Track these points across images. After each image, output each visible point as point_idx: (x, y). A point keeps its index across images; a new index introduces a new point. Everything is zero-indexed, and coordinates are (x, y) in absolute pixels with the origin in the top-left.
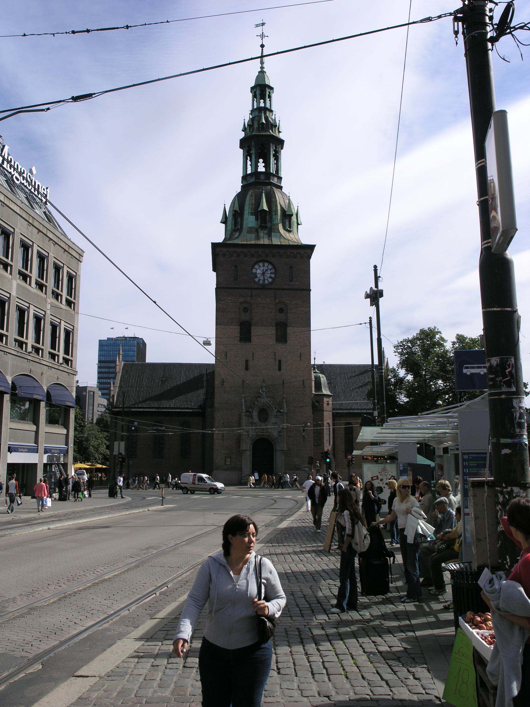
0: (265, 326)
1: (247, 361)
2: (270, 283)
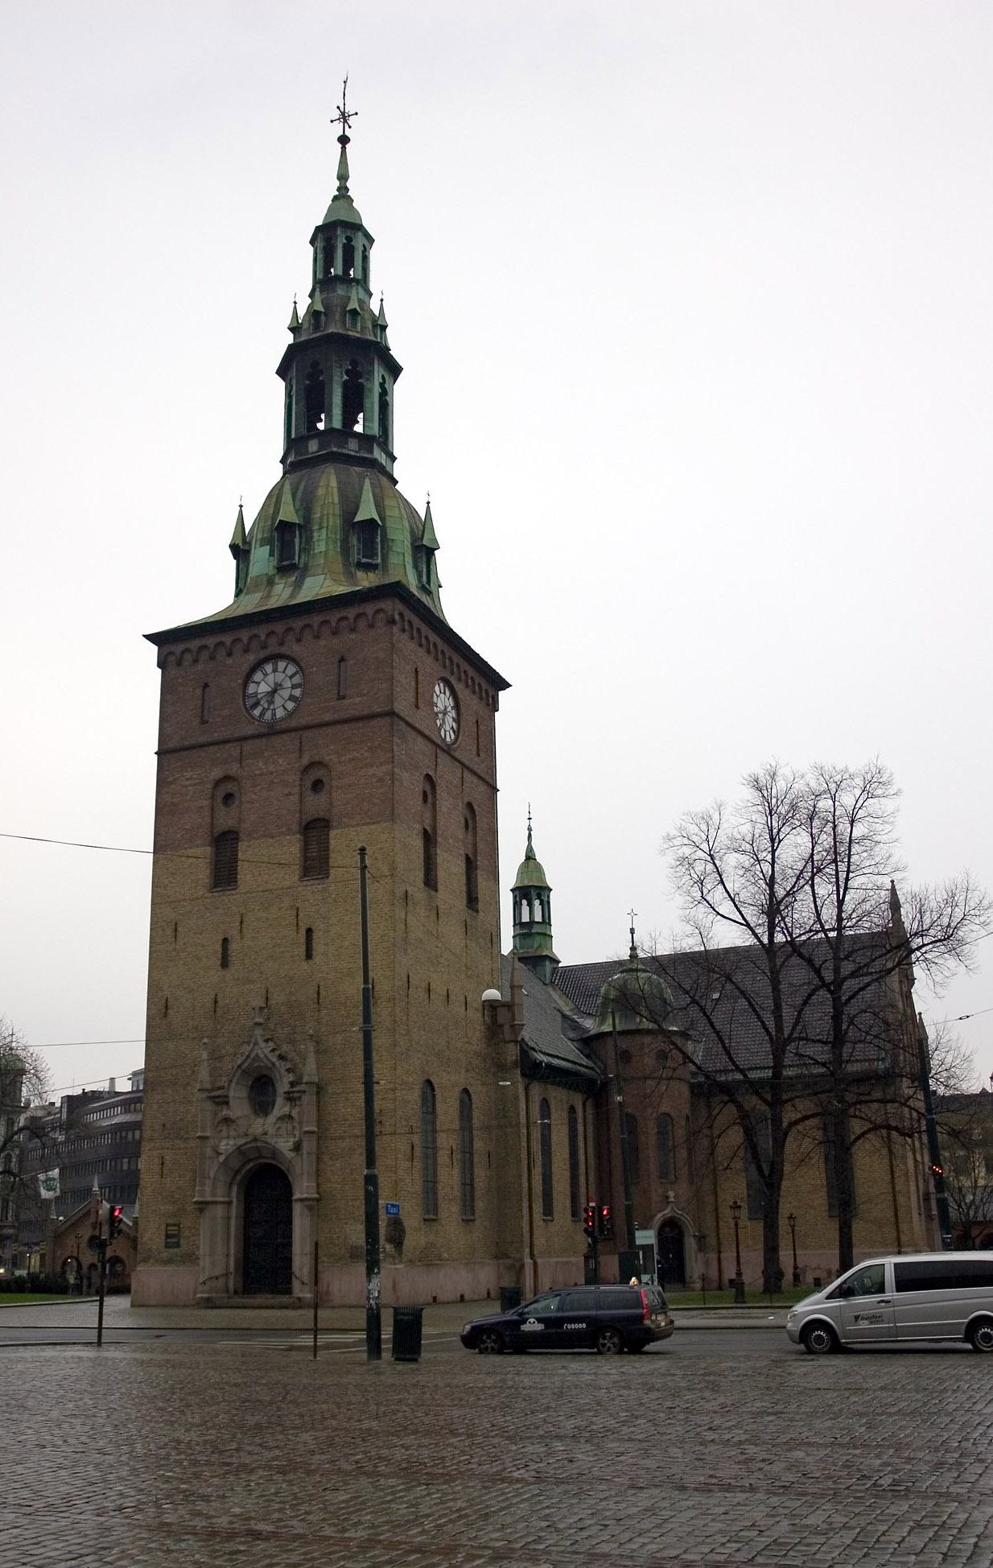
0: (273, 837)
1: (225, 941)
2: (290, 715)
